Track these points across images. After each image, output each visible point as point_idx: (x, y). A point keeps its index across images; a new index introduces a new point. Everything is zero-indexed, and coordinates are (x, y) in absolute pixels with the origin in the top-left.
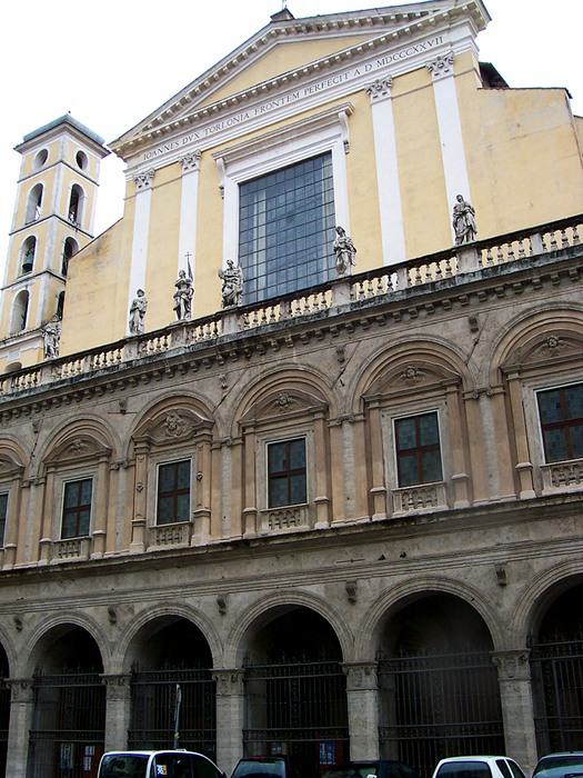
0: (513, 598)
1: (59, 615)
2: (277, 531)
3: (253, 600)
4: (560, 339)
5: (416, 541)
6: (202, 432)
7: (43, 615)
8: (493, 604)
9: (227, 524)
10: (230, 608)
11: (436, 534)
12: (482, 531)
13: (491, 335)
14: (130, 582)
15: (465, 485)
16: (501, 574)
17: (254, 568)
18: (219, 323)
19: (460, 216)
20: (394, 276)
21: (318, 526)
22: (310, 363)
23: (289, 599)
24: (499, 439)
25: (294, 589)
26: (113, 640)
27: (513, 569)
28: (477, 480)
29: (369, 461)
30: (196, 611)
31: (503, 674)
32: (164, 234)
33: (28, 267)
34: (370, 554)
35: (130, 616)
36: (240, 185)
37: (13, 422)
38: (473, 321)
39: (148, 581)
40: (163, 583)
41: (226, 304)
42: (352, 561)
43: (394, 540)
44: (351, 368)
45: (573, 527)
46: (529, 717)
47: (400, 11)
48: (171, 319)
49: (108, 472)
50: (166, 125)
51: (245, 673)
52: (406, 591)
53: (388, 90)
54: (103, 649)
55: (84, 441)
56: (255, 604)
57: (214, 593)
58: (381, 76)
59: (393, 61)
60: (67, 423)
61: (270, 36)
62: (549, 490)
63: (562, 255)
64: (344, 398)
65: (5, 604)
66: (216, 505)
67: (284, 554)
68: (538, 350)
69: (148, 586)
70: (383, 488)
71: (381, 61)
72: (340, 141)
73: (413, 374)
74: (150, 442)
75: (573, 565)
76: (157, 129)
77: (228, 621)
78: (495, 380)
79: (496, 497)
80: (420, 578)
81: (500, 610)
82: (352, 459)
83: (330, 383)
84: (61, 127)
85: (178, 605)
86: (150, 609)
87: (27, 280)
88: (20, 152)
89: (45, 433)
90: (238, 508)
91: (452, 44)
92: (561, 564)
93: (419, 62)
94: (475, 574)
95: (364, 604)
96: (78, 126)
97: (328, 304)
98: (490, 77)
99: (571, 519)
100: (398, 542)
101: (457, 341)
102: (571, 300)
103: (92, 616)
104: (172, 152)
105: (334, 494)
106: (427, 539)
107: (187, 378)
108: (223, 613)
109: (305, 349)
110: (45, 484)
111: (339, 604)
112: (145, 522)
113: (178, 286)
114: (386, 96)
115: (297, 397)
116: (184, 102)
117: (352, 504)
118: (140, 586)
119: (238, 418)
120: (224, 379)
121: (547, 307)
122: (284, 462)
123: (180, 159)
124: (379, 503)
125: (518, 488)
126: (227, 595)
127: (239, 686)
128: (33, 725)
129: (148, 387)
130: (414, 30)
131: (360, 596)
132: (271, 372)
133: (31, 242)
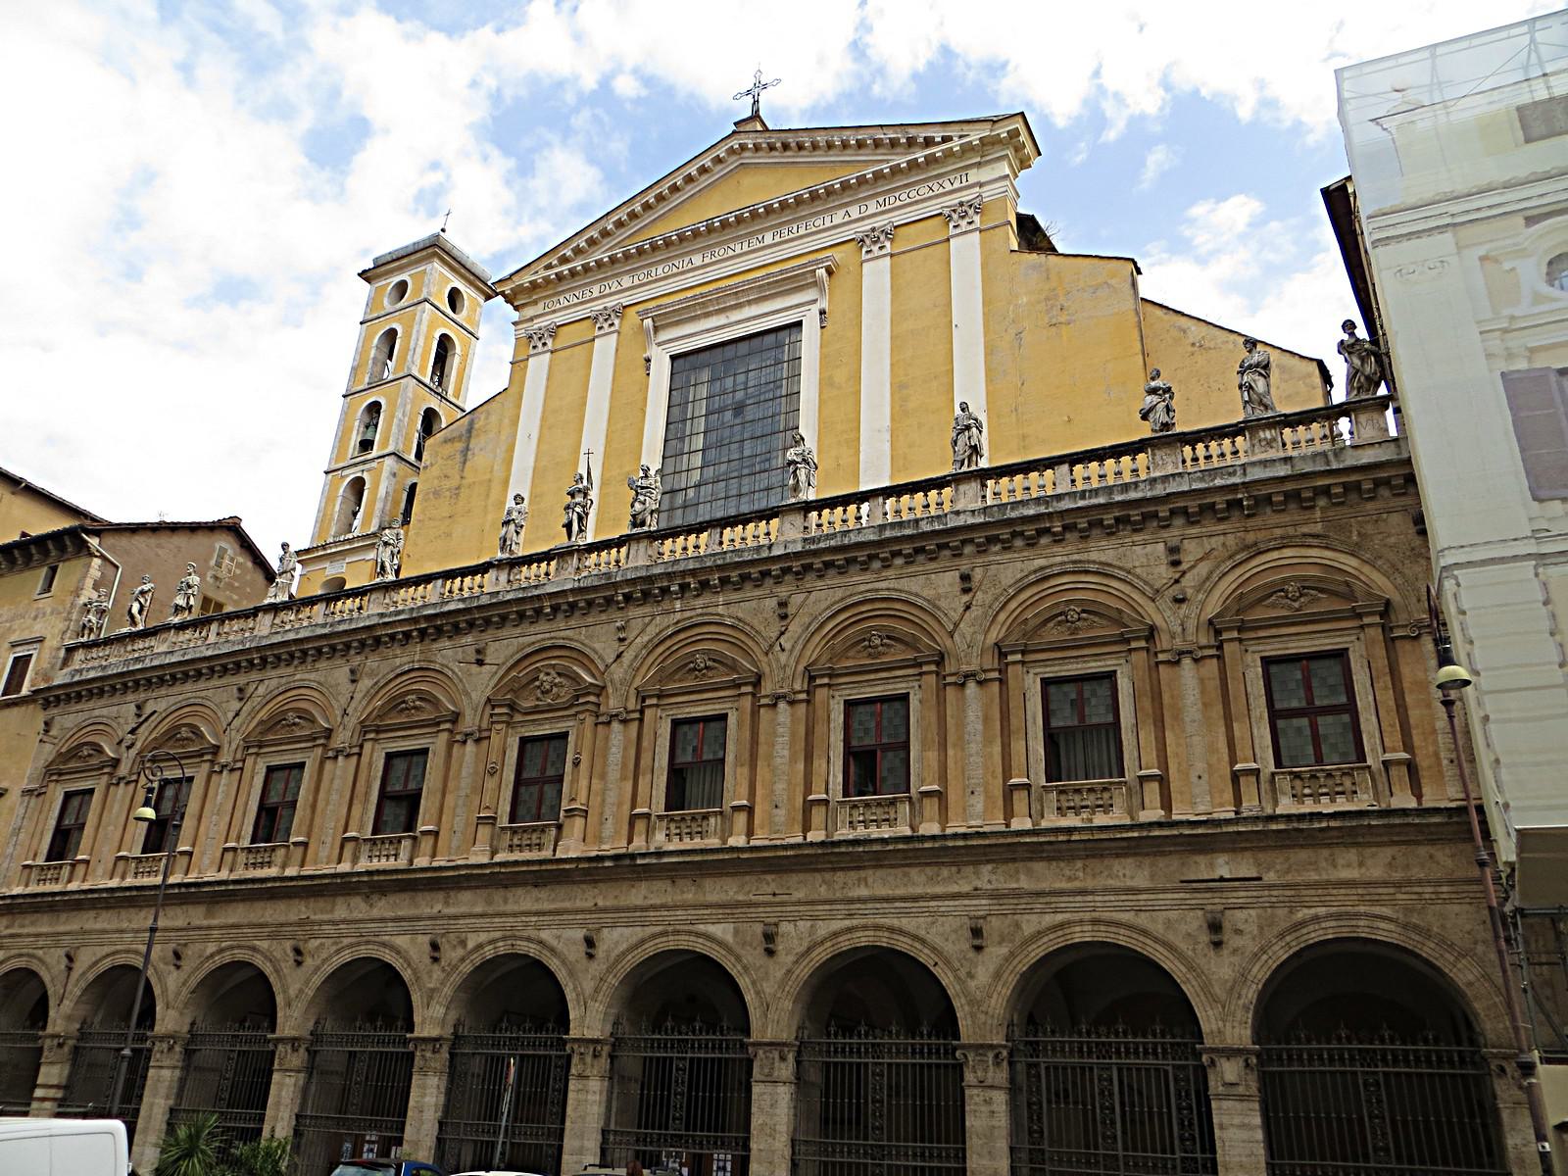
0: (992, 968)
1: (359, 944)
2: (674, 845)
3: (634, 940)
4: (1084, 611)
5: (862, 873)
6: (586, 698)
7: (336, 943)
8: (962, 973)
9: (608, 829)
10: (600, 951)
11: (892, 866)
12: (954, 869)
13: (989, 598)
14: (466, 902)
15: (936, 800)
16: (977, 932)
17: (638, 894)
18: (624, 550)
19: (962, 431)
20: (865, 507)
21: (732, 842)
22: (740, 615)
23: (684, 943)
24: (988, 741)
25: (691, 927)
26: (431, 986)
27: (994, 926)
28: (953, 797)
29: (809, 759)
30: (552, 950)
31: (969, 1077)
32: (562, 417)
33: (366, 445)
34: (801, 887)
35: (460, 952)
36: (673, 358)
37: (322, 664)
38: (965, 578)
39: (489, 903)
40: (510, 907)
41: (634, 525)
42: (774, 895)
43: (834, 870)
44: (795, 628)
45: (1081, 874)
46: (1002, 1145)
47: (912, 132)
48: (561, 540)
49: (450, 744)
50: (577, 264)
51: (613, 1045)
52: (845, 944)
53: (888, 244)
54: (416, 998)
55: (420, 699)
56: (636, 946)
57: (582, 925)
58: (880, 222)
59: (898, 203)
60: (398, 671)
61: (731, 151)
62: (1051, 821)
63: (1097, 495)
64: (782, 669)
65: (282, 925)
66: (595, 801)
67: (685, 877)
68: (1051, 624)
69: (490, 910)
70: (824, 796)
71: (881, 200)
72: (815, 309)
73: (878, 642)
74: (512, 707)
75: (1078, 929)
76: (565, 268)
77: (596, 968)
78: (991, 662)
79: (978, 822)
80: (865, 928)
81: (972, 984)
82: (786, 753)
83: (765, 646)
84: (430, 250)
85: (529, 939)
86: (490, 942)
87: (364, 462)
88: (368, 280)
89: (366, 683)
90: (627, 806)
91: (981, 185)
92: (1061, 926)
93: (933, 207)
94: (941, 929)
95: (785, 959)
96: (455, 253)
97: (773, 537)
98: (1031, 234)
99: (1079, 864)
100: (839, 874)
101: (943, 604)
102: (1103, 559)
103: (406, 950)
104: (582, 303)
105: (758, 799)
106: (880, 873)
107: (573, 623)
108: (590, 956)
109: (735, 596)
110: (360, 755)
111: (754, 956)
112: (495, 819)
113: (572, 495)
114: (884, 252)
115: (719, 660)
116: (605, 234)
117: (781, 814)
118: (478, 909)
119: (637, 682)
120: (622, 629)
121: (1070, 567)
122: (695, 749)
123: (593, 314)
124: (818, 815)
125: (1009, 814)
126: (599, 930)
127: (604, 1062)
128: (303, 1105)
129: (518, 631)
130: (931, 160)
131: (780, 946)
132: (687, 623)
133: (374, 408)
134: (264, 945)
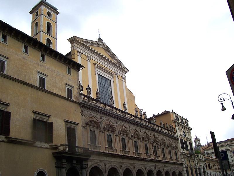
50: (84, 43)
58: (118, 73)
134: (130, 166)
